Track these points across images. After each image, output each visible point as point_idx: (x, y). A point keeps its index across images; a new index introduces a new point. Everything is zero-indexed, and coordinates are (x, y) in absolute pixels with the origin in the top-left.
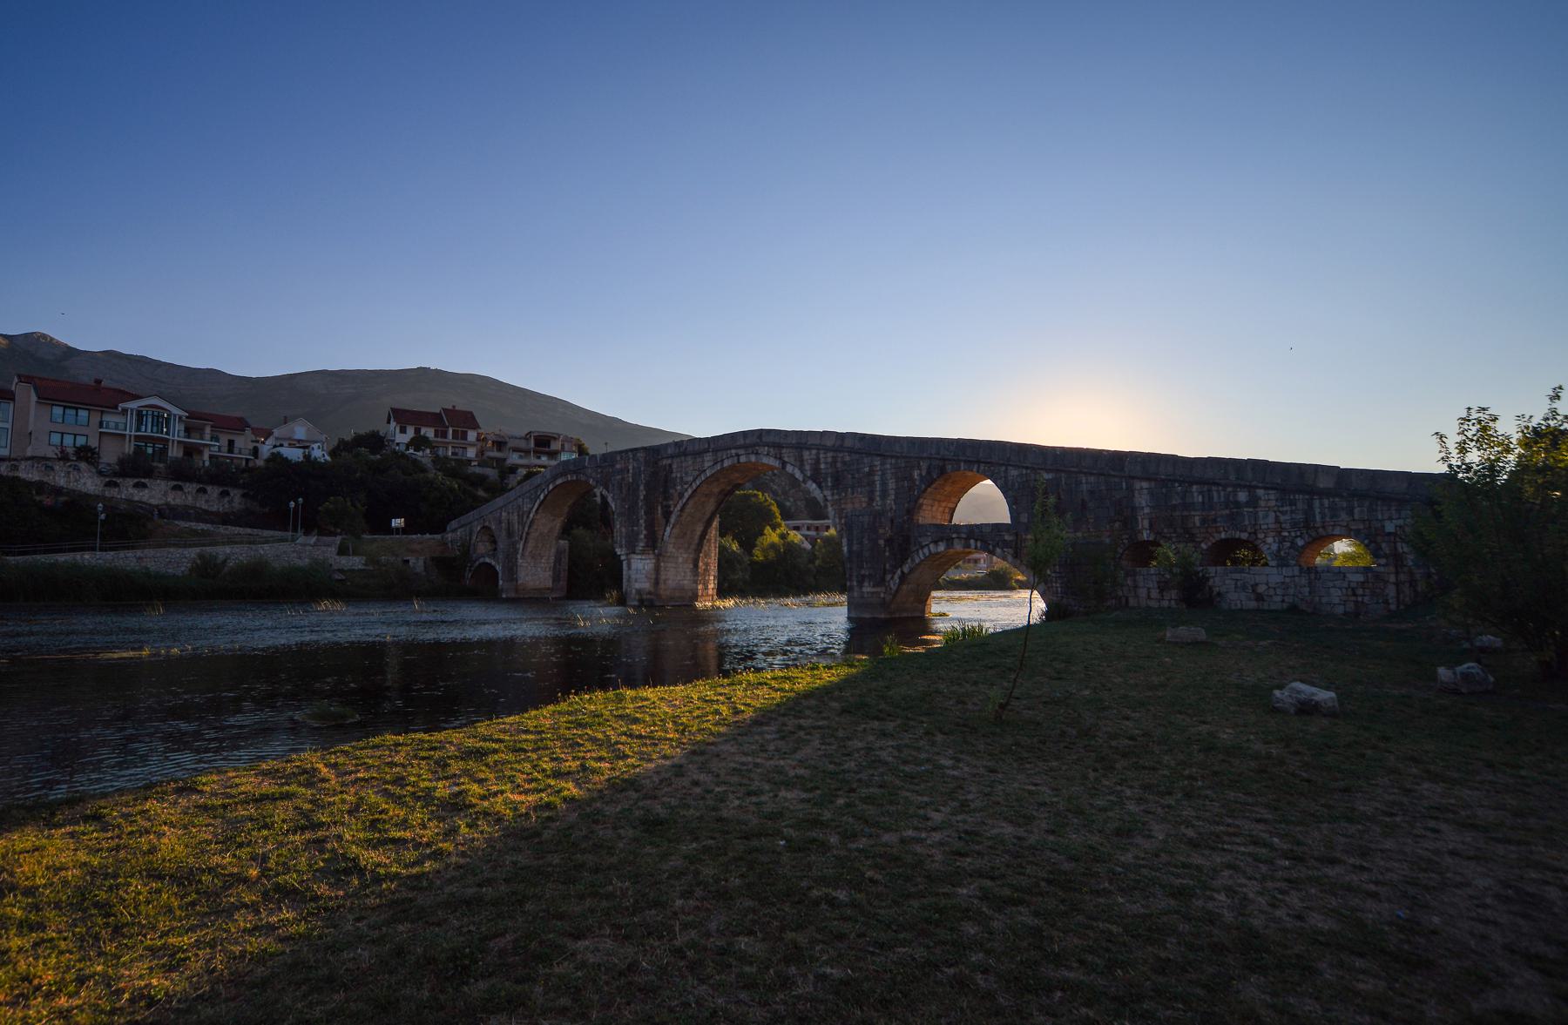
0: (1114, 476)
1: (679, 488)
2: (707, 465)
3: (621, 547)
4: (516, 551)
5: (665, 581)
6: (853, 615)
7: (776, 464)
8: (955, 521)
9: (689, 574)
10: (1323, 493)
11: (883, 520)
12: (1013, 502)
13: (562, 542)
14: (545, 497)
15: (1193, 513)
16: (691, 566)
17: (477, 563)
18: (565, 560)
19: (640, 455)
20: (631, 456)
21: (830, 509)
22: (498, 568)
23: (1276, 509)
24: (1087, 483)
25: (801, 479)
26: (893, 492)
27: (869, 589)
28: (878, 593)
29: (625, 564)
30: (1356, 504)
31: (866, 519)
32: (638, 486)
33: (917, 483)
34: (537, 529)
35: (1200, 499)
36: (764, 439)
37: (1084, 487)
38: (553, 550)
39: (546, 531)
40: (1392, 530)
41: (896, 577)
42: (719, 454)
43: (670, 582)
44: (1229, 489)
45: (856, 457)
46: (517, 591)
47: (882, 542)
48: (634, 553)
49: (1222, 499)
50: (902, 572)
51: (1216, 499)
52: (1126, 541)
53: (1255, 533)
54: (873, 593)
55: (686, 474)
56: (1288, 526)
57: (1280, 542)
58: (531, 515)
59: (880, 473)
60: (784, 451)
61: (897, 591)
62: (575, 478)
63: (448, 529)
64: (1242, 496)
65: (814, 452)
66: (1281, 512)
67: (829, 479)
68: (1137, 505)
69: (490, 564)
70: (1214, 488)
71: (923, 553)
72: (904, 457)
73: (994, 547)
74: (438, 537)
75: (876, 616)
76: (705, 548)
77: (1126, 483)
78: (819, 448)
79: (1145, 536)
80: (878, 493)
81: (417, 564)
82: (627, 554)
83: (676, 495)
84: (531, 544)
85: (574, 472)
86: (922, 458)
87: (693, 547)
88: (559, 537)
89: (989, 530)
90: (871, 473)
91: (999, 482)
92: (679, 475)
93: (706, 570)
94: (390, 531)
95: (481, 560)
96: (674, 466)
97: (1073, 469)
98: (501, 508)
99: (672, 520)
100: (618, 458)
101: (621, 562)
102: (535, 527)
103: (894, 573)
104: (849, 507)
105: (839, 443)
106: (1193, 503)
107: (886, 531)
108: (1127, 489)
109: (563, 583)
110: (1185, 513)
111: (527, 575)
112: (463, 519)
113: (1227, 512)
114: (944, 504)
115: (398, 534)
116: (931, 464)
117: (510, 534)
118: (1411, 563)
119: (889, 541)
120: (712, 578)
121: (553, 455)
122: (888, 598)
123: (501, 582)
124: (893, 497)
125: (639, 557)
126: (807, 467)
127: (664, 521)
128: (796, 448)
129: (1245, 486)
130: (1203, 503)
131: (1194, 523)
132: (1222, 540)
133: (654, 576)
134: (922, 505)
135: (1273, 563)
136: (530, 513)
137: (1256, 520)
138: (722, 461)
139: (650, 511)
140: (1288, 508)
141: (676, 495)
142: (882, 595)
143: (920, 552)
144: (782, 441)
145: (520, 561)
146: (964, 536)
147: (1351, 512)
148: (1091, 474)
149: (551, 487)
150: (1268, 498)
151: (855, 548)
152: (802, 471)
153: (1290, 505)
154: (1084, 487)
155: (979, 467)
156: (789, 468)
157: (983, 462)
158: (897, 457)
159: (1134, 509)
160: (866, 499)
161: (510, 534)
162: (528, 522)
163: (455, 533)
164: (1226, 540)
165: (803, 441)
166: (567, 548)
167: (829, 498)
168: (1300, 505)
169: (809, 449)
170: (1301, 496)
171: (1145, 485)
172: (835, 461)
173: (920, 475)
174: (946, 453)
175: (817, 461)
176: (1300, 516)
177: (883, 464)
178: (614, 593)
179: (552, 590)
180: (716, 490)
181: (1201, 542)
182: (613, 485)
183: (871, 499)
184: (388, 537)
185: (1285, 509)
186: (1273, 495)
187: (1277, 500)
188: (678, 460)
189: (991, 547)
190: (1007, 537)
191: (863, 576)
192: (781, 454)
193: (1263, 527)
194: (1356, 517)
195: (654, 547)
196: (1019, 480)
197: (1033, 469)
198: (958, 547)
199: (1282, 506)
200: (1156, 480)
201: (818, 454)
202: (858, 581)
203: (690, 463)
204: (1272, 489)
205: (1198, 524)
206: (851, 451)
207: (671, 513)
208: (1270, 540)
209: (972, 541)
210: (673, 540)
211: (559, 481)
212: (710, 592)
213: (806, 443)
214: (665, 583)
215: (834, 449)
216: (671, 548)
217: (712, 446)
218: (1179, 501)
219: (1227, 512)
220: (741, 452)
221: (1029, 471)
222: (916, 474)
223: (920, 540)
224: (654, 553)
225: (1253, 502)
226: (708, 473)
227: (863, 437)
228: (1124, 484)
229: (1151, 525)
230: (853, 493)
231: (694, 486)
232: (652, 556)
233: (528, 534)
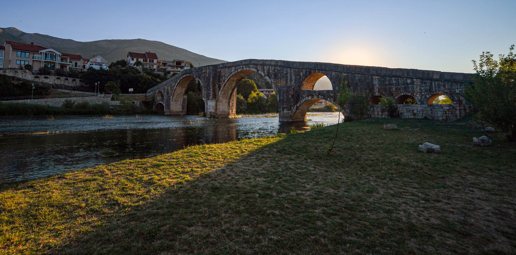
0: (367, 75)
1: (223, 78)
2: (233, 71)
3: (204, 98)
4: (170, 99)
5: (219, 109)
6: (281, 120)
7: (255, 70)
8: (314, 89)
9: (227, 107)
10: (436, 80)
11: (291, 89)
12: (333, 83)
13: (185, 96)
14: (180, 81)
15: (393, 87)
16: (228, 104)
17: (157, 103)
18: (186, 102)
19: (211, 68)
20: (208, 68)
21: (273, 85)
22: (164, 105)
23: (420, 85)
24: (358, 77)
25: (264, 75)
26: (294, 80)
27: (286, 112)
28: (289, 113)
29: (206, 104)
30: (446, 84)
31: (285, 89)
32: (210, 78)
33: (302, 77)
34: (176, 92)
35: (395, 82)
36: (251, 62)
37: (357, 78)
38: (182, 99)
39: (180, 92)
40: (458, 92)
41: (295, 108)
42: (237, 67)
43: (220, 109)
44: (405, 79)
45: (281, 68)
46: (170, 112)
47: (290, 96)
48: (209, 100)
49: (402, 82)
50: (297, 106)
51: (400, 82)
52: (370, 96)
53: (413, 93)
54: (287, 113)
56: (424, 91)
57: (421, 96)
58: (175, 87)
59: (289, 73)
60: (258, 66)
61: (295, 112)
62: (189, 75)
63: (148, 92)
64: (409, 81)
65: (268, 66)
66: (421, 86)
67: (273, 76)
68: (374, 84)
69: (161, 104)
70: (399, 78)
71: (304, 100)
72: (298, 68)
73: (327, 98)
74: (144, 94)
75: (288, 120)
76: (232, 98)
77: (371, 77)
78: (270, 65)
80: (289, 80)
81: (137, 103)
82: (206, 100)
83: (222, 81)
84: (175, 97)
85: (189, 73)
86: (304, 69)
87: (228, 98)
88: (184, 95)
89: (325, 92)
90: (287, 73)
91: (329, 76)
93: (232, 106)
94: (128, 92)
95: (158, 102)
96: (222, 71)
97: (353, 72)
98: (165, 85)
99: (221, 89)
100: (203, 69)
101: (204, 103)
102: (176, 91)
103: (294, 106)
104: (280, 84)
105: (276, 64)
106: (393, 83)
107: (292, 92)
108: (371, 79)
109: (185, 110)
110: (390, 87)
111: (173, 107)
112: (152, 89)
113: (404, 86)
114: (311, 84)
115: (131, 93)
116: (306, 71)
117: (168, 94)
118: (464, 103)
119: (293, 96)
120: (234, 108)
121: (182, 67)
122: (292, 115)
123: (165, 109)
124: (294, 81)
125: (210, 101)
126: (266, 72)
127: (218, 89)
128: (262, 65)
129: (410, 78)
130: (396, 83)
131: (393, 90)
132: (402, 96)
133: (215, 107)
134: (303, 84)
135: (419, 103)
136: (174, 87)
137: (413, 89)
138: (238, 69)
139: (214, 86)
140: (424, 85)
142: (290, 114)
143: (303, 99)
144: (257, 63)
145: (171, 102)
146: (317, 94)
147: (444, 86)
148: (359, 74)
149: (181, 78)
150: (417, 82)
151: (281, 98)
152: (264, 73)
153: (425, 84)
154: (357, 78)
155: (322, 72)
156: (260, 72)
157: (324, 70)
158: (296, 68)
159: (373, 85)
160: (285, 82)
161: (168, 94)
162: (174, 90)
163: (150, 93)
164: (404, 96)
165: (264, 63)
166: (187, 98)
167: (273, 82)
168: (428, 84)
169: (266, 66)
170: (428, 81)
171: (377, 77)
173: (303, 74)
174: (312, 67)
175: (269, 70)
176: (428, 88)
177: (290, 70)
178: (202, 113)
179: (182, 112)
180: (236, 79)
181: (395, 96)
182: (202, 78)
183: (287, 82)
184: (128, 94)
185: (423, 85)
186: (419, 80)
187: (420, 82)
188: (223, 69)
189: (326, 98)
190: (331, 95)
191: (284, 108)
192: (257, 67)
193: (416, 91)
194: (446, 88)
195: (215, 98)
196: (335, 76)
197: (340, 72)
198: (315, 98)
199: (422, 84)
200: (380, 76)
201: (269, 67)
202: (282, 109)
203: (227, 70)
204: (419, 79)
205: (394, 90)
206: (280, 66)
207: (221, 86)
208: (418, 95)
209: (320, 96)
210: (221, 96)
211: (184, 76)
212: (234, 113)
213: (265, 64)
214: (219, 110)
215: (276, 66)
216: (221, 98)
217: (234, 65)
218: (388, 83)
219: (404, 86)
220: (244, 66)
221: (339, 73)
222: (301, 74)
223: (303, 95)
224: (215, 100)
225: (412, 83)
226: (233, 74)
227: (284, 62)
228: (370, 77)
229: (379, 91)
230: (281, 80)
231: (228, 78)
232: (215, 101)
233: (174, 93)
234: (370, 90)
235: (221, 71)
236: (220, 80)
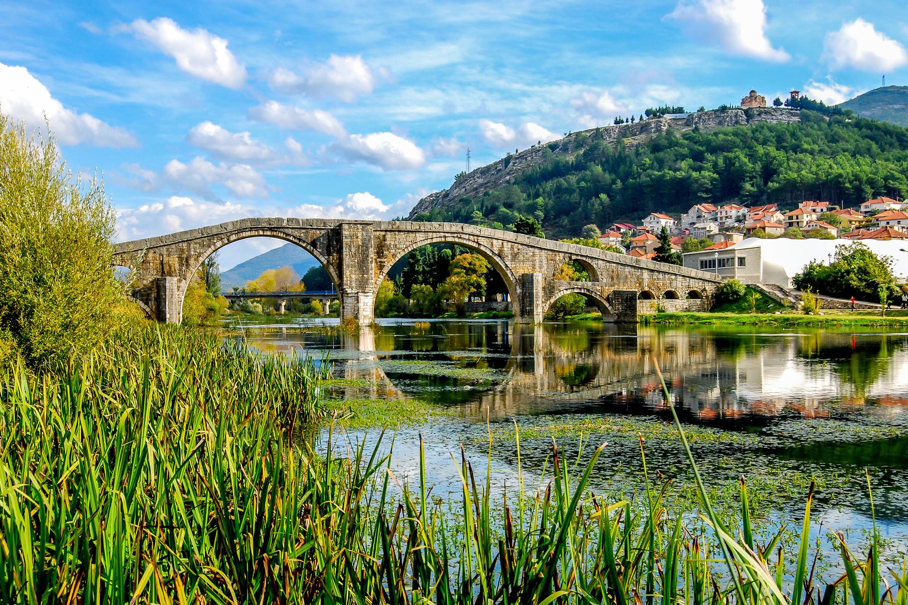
1: (393, 251)
42: (430, 235)
55: (400, 244)
60: (480, 238)
79: (646, 289)
83: (390, 255)
90: (534, 255)
92: (393, 243)
119: (544, 288)
141: (390, 255)
172: (512, 248)
183: (534, 268)
197: (609, 262)
206: (522, 245)
207: (384, 266)
217: (422, 228)
220: (447, 235)
222: (557, 258)
231: (407, 251)
234: (640, 284)
235: (384, 236)
236: (383, 253)
